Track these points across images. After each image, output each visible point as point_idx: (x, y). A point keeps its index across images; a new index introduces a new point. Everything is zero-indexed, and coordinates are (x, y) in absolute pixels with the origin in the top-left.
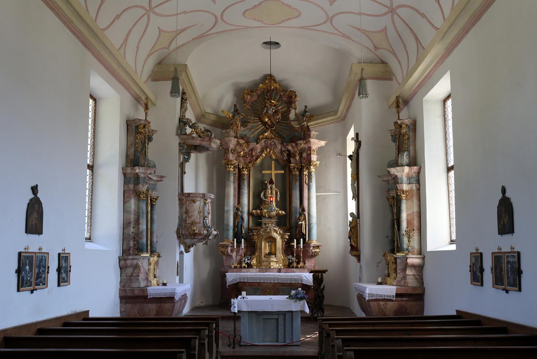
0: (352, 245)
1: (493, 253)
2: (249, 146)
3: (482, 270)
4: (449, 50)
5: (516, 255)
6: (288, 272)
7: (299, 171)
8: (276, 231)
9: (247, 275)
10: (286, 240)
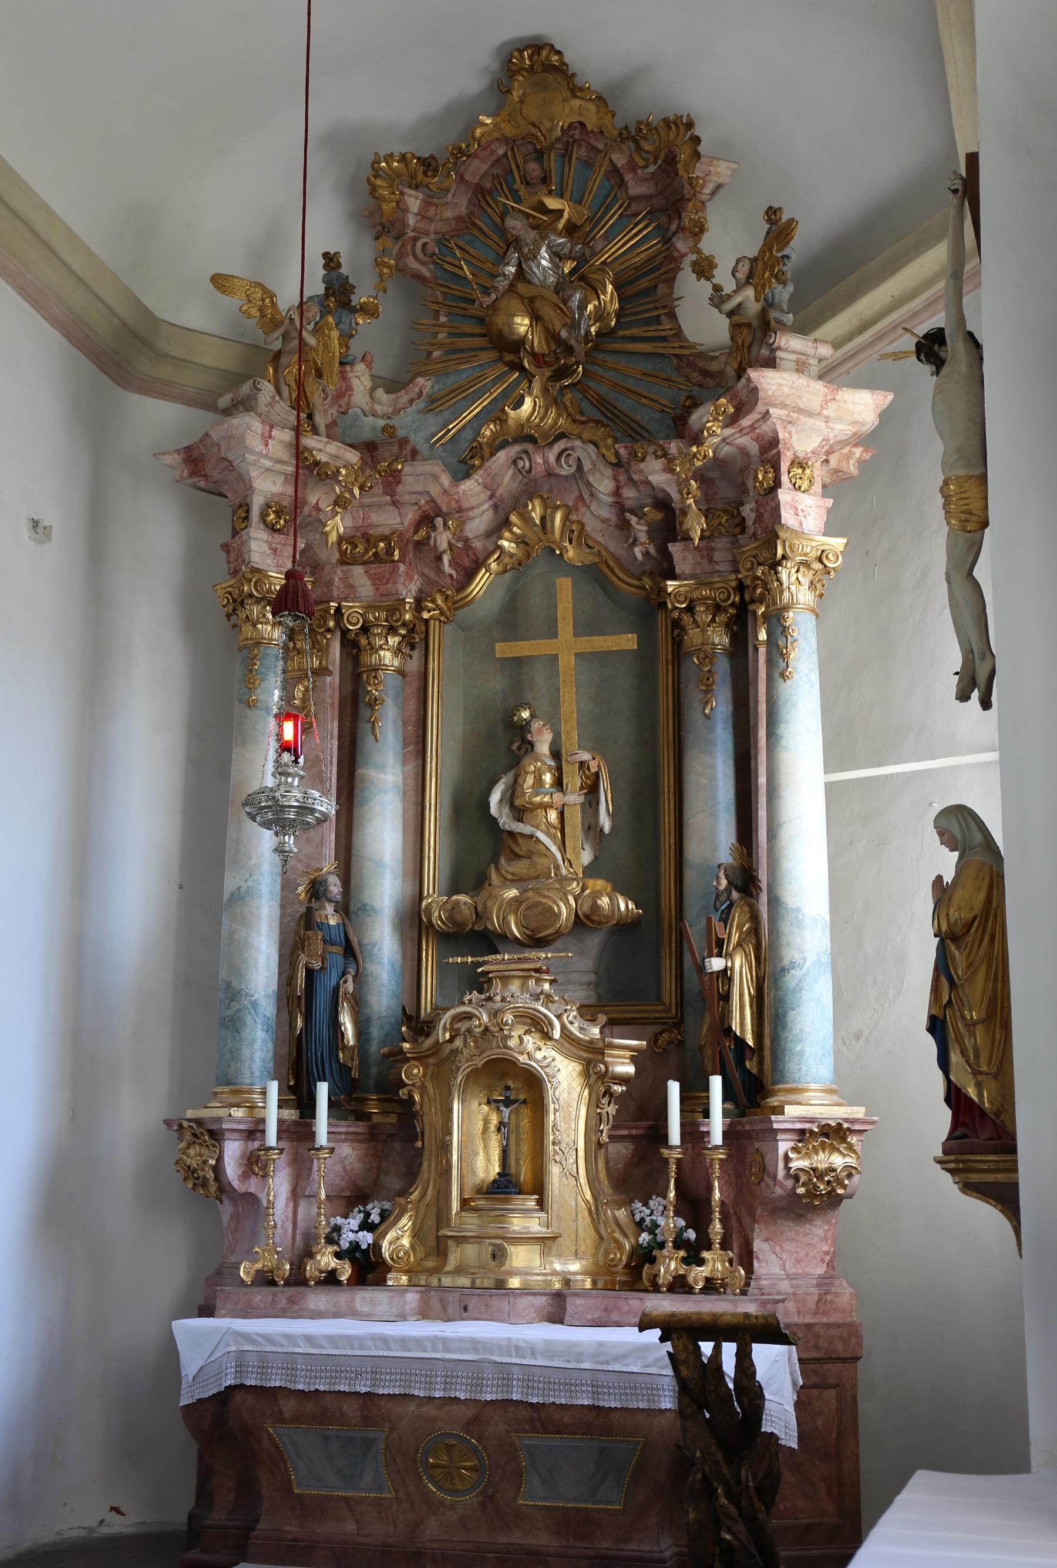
0: (958, 1091)
2: (400, 489)
6: (615, 1317)
7: (728, 626)
8: (539, 1026)
9: (286, 1336)
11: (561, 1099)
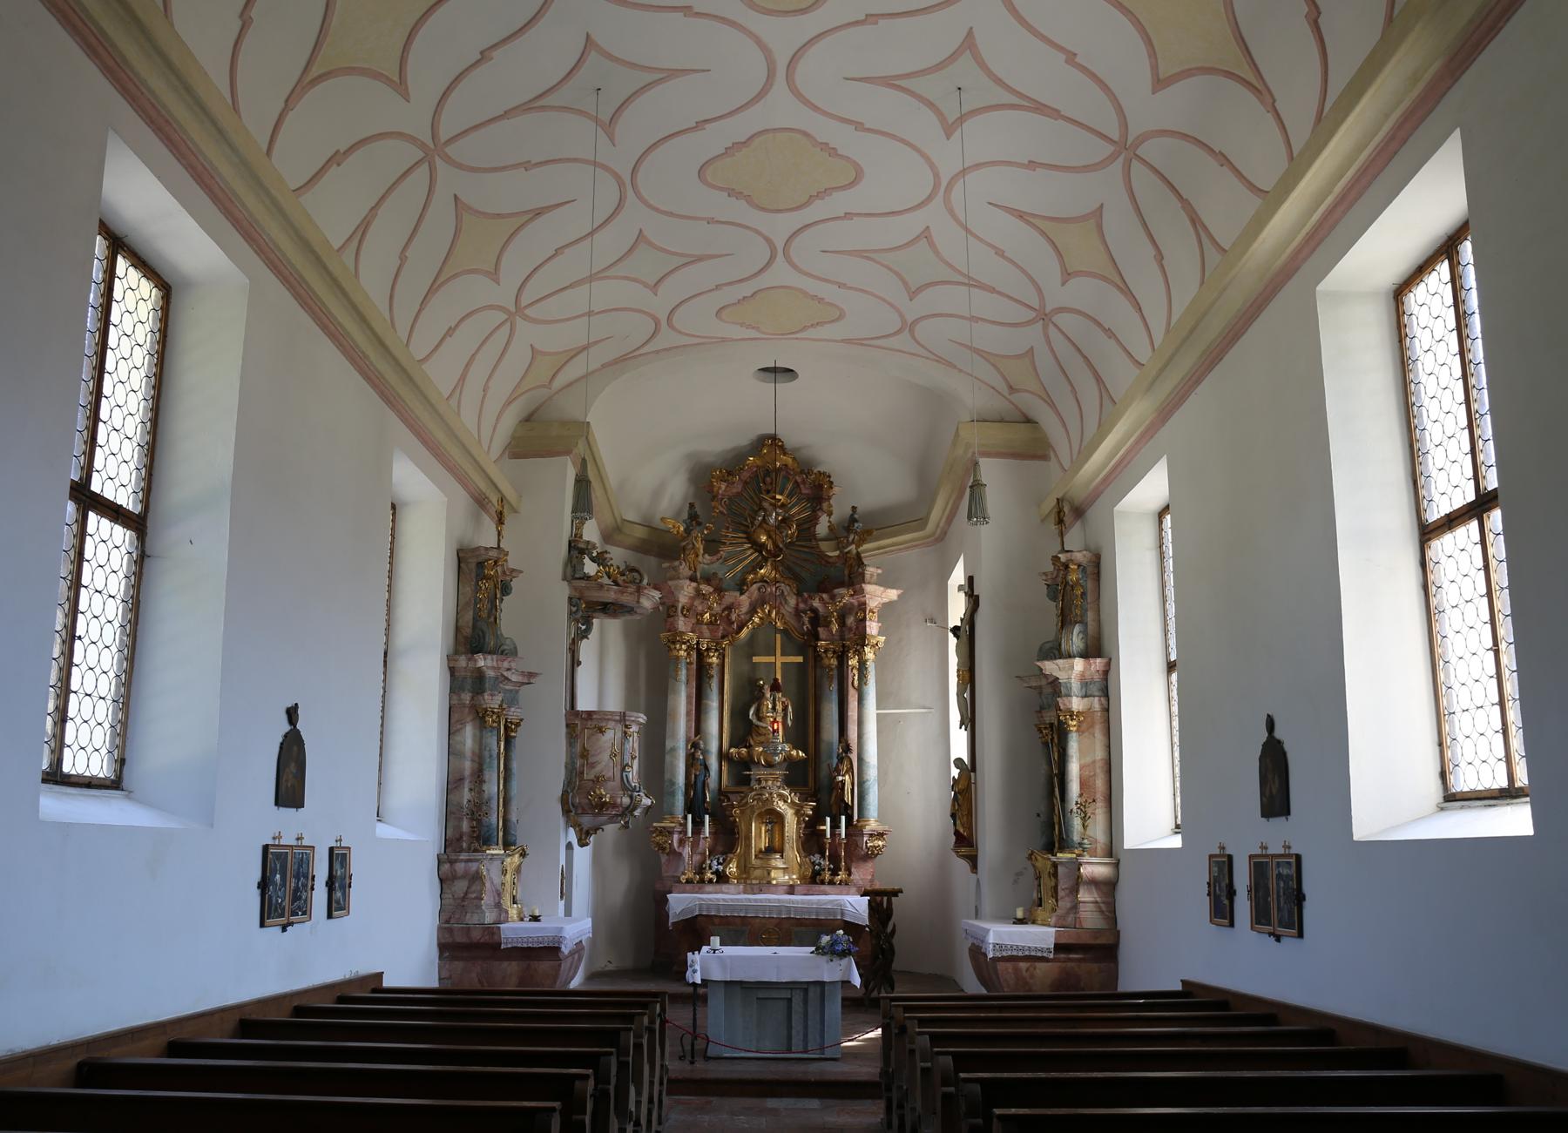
1: (1251, 857)
3: (1231, 893)
4: (1165, 414)
5: (1293, 860)
6: (811, 893)
7: (838, 658)
8: (783, 798)
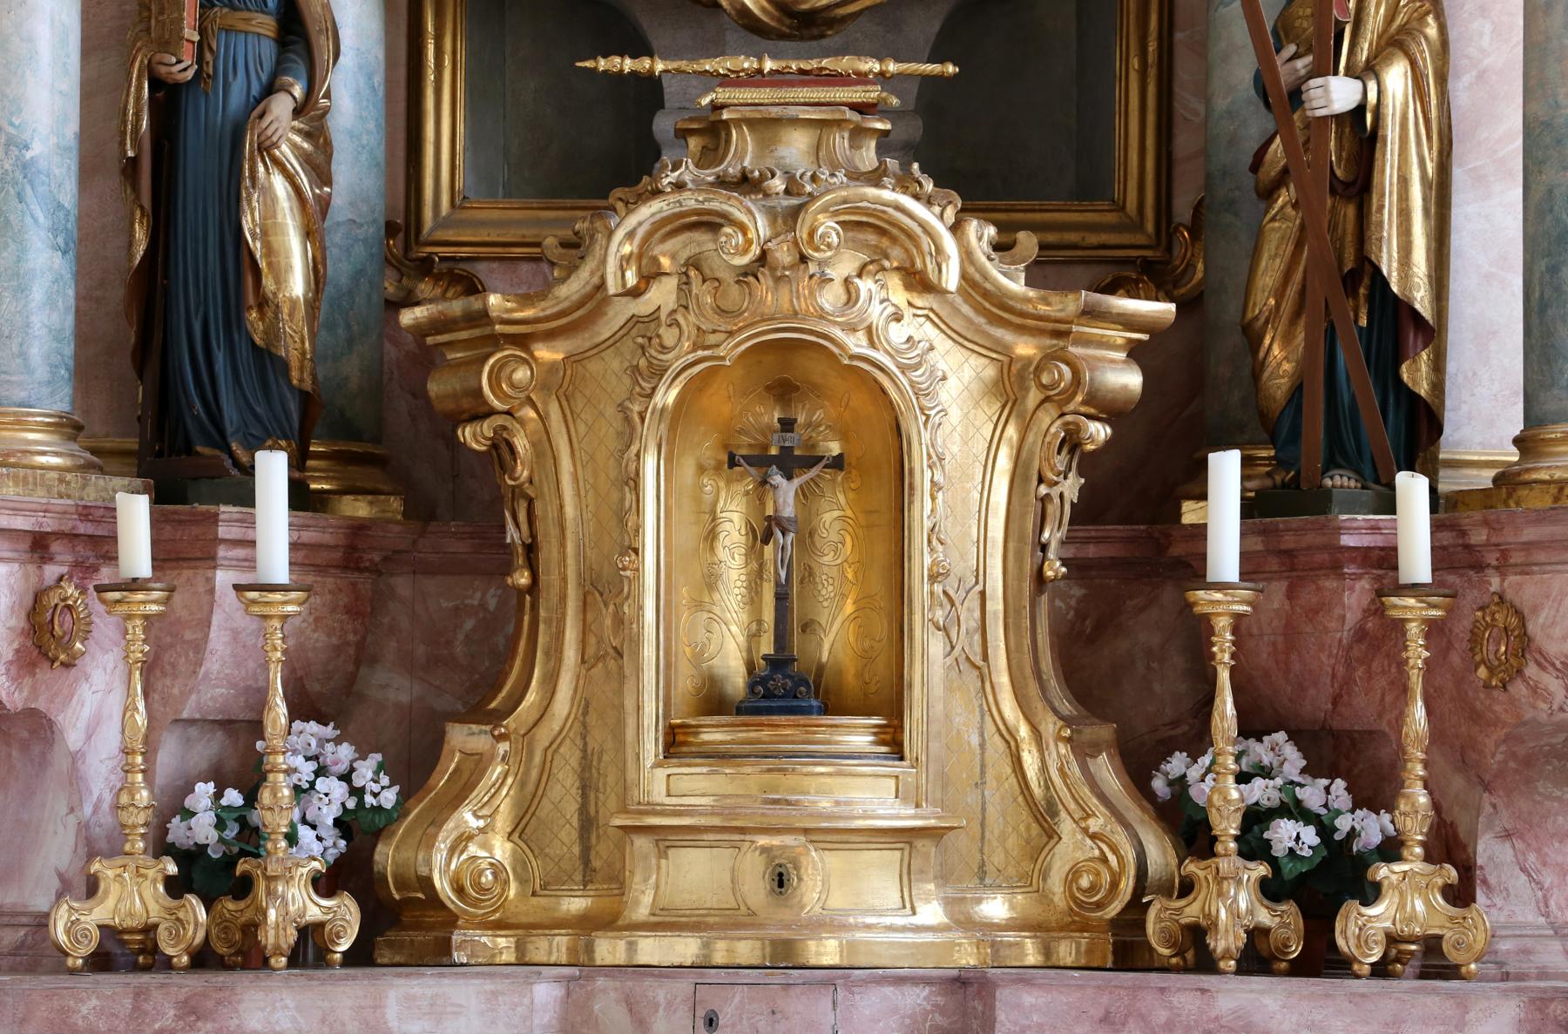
10: (1099, 432)
11: (948, 458)
